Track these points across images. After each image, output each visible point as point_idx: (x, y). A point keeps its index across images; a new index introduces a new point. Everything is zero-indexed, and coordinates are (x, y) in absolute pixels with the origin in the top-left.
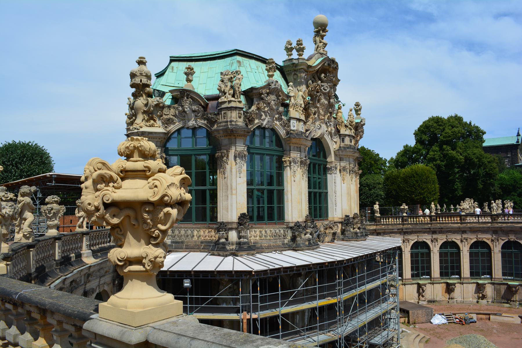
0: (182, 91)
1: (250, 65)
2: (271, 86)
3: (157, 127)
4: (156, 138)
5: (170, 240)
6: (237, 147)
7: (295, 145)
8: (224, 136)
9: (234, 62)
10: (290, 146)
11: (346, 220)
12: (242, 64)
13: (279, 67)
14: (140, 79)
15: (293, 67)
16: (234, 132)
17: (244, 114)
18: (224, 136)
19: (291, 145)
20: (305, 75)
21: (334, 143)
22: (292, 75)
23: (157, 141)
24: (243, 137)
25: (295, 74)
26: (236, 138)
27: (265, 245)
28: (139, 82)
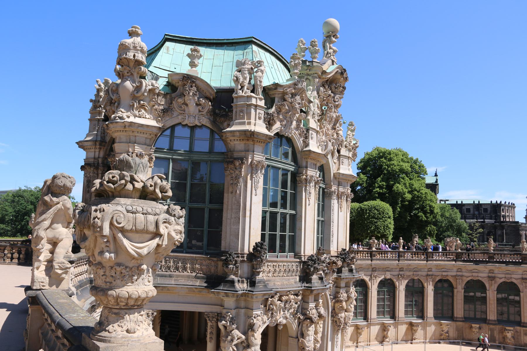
4: (146, 133)
6: (255, 156)
8: (240, 140)
9: (249, 52)
10: (307, 162)
11: (343, 254)
15: (307, 70)
18: (240, 140)
21: (334, 164)
23: (146, 138)
25: (307, 79)
26: (254, 145)
27: (278, 283)
28: (132, 57)
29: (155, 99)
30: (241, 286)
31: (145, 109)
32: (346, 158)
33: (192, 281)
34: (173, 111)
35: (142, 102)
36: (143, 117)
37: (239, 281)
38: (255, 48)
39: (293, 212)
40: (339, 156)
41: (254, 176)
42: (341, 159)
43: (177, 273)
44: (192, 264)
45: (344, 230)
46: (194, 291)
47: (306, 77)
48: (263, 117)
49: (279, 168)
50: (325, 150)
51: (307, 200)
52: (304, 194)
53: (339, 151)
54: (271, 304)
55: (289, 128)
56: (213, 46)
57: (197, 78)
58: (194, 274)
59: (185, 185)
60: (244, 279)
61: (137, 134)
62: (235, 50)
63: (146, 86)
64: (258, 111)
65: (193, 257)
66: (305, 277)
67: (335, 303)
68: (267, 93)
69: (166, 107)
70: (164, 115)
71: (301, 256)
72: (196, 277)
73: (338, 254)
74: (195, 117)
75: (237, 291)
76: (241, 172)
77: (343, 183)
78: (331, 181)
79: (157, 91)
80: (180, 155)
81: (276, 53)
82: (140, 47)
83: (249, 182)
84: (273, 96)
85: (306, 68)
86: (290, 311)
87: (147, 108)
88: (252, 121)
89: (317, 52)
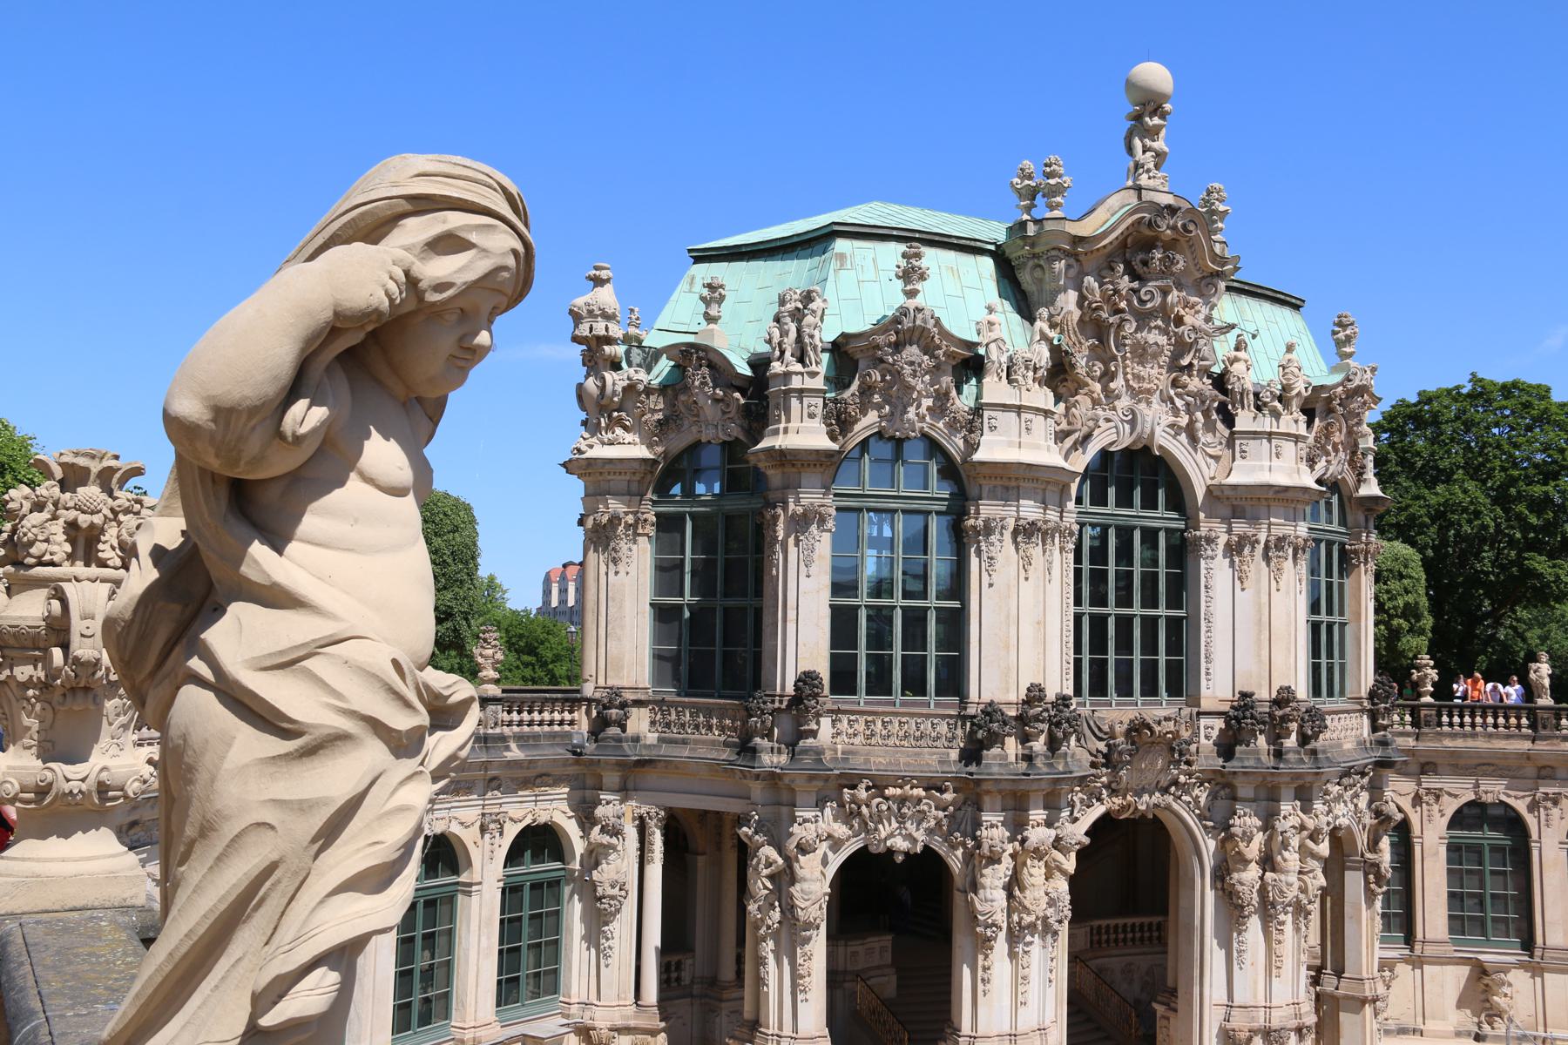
0: (685, 351)
1: (874, 260)
2: (900, 323)
3: (629, 443)
5: (656, 735)
7: (994, 482)
10: (980, 486)
12: (849, 262)
13: (992, 248)
14: (588, 325)
16: (788, 457)
17: (825, 405)
19: (983, 482)
20: (1068, 267)
22: (1028, 269)
24: (819, 469)
26: (800, 473)
27: (880, 759)
28: (587, 333)
29: (642, 402)
30: (775, 760)
31: (625, 428)
32: (1254, 439)
33: (718, 751)
34: (681, 419)
35: (615, 414)
36: (619, 443)
37: (772, 749)
38: (841, 245)
39: (955, 604)
40: (1233, 433)
41: (801, 538)
42: (1238, 442)
43: (697, 736)
44: (721, 719)
45: (1259, 640)
46: (717, 771)
47: (1031, 263)
48: (819, 411)
49: (895, 511)
50: (1131, 434)
51: (985, 575)
52: (974, 561)
53: (1229, 421)
54: (853, 801)
55: (902, 420)
56: (778, 254)
57: (706, 349)
58: (723, 738)
59: (716, 560)
60: (783, 746)
61: (609, 477)
62: (811, 256)
63: (614, 384)
64: (806, 401)
65: (720, 704)
66: (972, 753)
67: (1223, 841)
68: (846, 352)
69: (668, 413)
70: (661, 430)
71: (967, 703)
72: (726, 744)
73: (1232, 707)
74: (716, 426)
75: (754, 768)
76: (775, 532)
77: (1248, 509)
78: (1197, 510)
79: (641, 387)
80: (704, 503)
81: (917, 235)
82: (600, 309)
83: (792, 550)
84: (855, 358)
85: (1020, 243)
86: (925, 825)
87: (627, 423)
88: (793, 425)
89: (1058, 190)
